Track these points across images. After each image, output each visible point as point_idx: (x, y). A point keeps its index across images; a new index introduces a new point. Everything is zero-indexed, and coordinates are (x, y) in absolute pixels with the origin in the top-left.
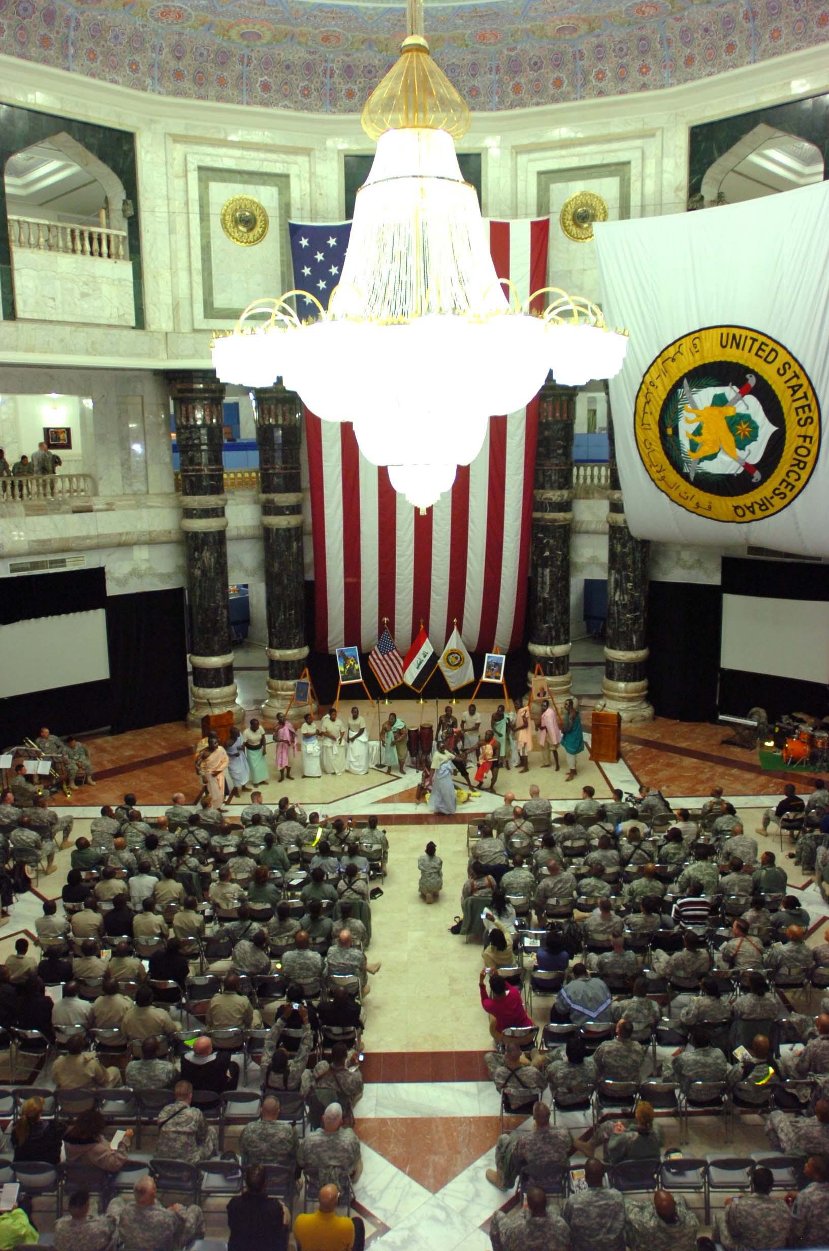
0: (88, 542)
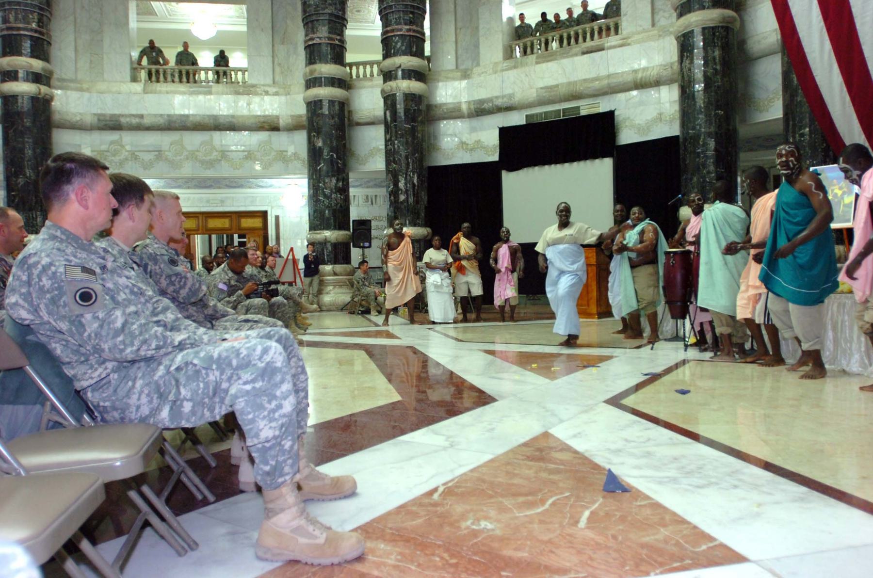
0: (597, 84)
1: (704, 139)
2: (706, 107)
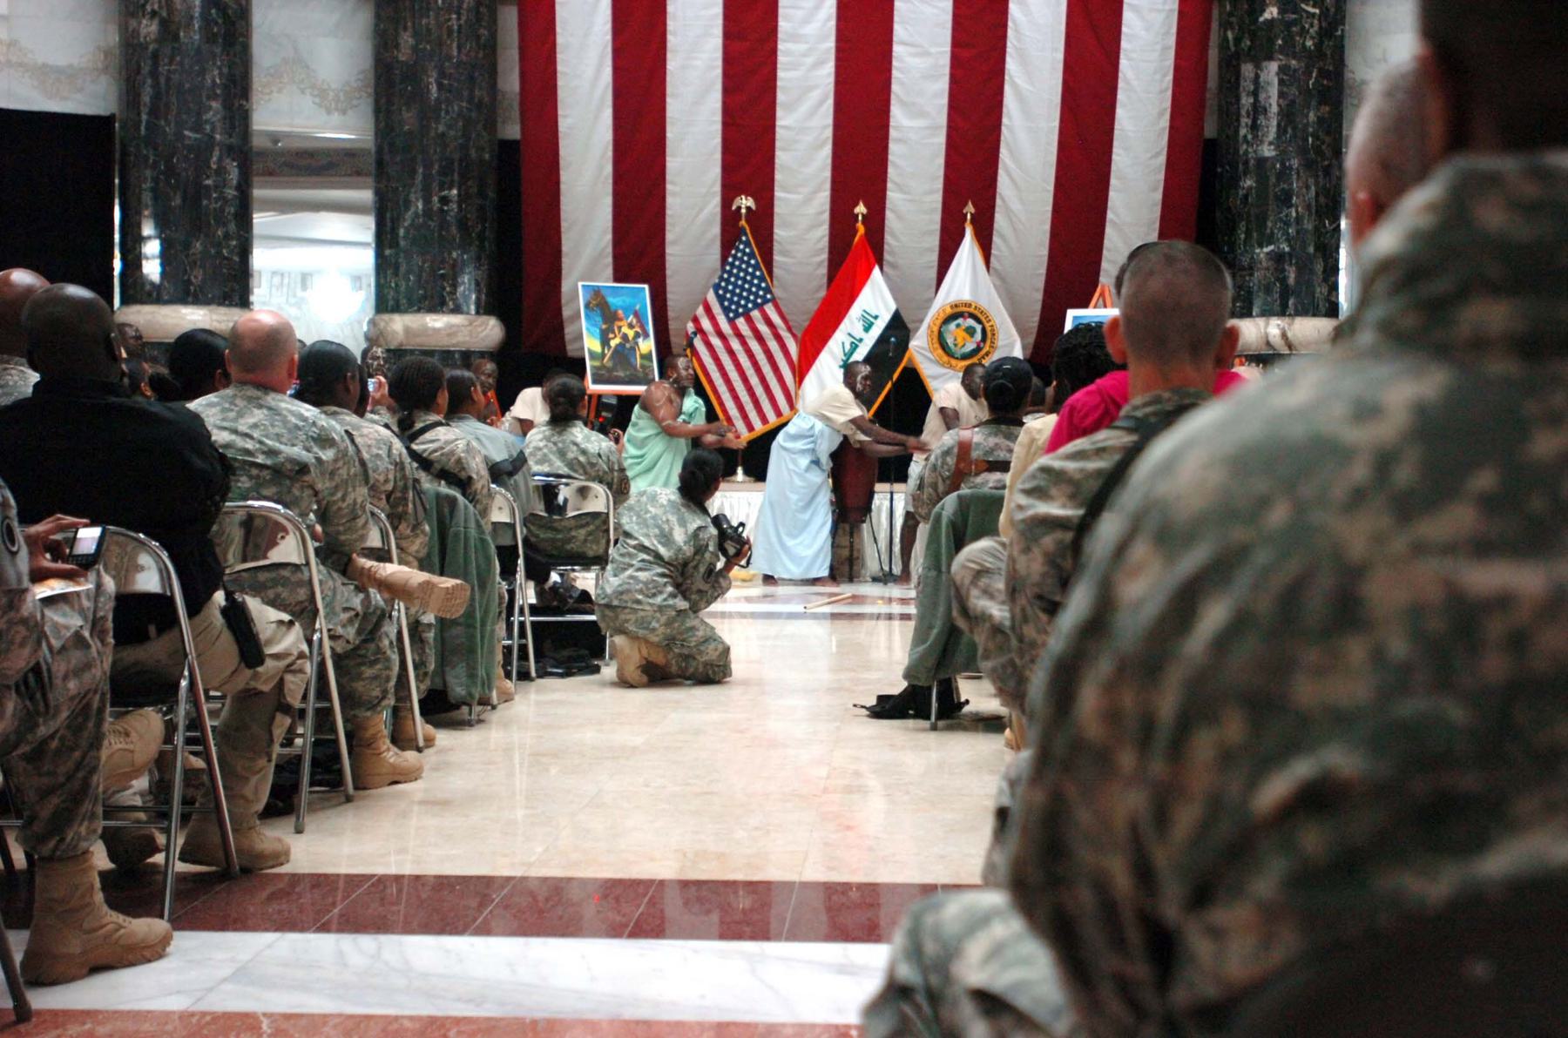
1: (220, 159)
2: (225, 87)
